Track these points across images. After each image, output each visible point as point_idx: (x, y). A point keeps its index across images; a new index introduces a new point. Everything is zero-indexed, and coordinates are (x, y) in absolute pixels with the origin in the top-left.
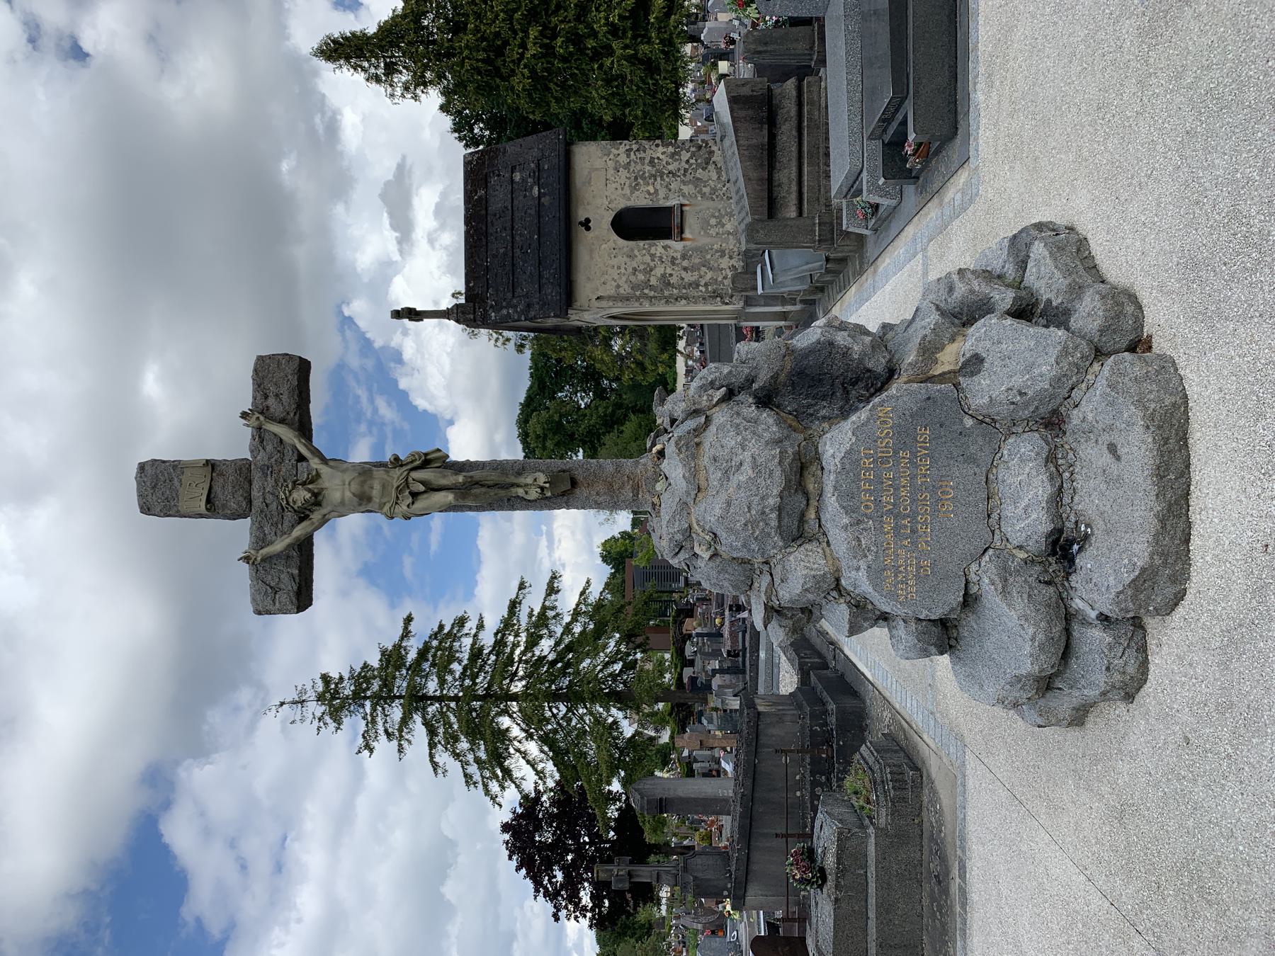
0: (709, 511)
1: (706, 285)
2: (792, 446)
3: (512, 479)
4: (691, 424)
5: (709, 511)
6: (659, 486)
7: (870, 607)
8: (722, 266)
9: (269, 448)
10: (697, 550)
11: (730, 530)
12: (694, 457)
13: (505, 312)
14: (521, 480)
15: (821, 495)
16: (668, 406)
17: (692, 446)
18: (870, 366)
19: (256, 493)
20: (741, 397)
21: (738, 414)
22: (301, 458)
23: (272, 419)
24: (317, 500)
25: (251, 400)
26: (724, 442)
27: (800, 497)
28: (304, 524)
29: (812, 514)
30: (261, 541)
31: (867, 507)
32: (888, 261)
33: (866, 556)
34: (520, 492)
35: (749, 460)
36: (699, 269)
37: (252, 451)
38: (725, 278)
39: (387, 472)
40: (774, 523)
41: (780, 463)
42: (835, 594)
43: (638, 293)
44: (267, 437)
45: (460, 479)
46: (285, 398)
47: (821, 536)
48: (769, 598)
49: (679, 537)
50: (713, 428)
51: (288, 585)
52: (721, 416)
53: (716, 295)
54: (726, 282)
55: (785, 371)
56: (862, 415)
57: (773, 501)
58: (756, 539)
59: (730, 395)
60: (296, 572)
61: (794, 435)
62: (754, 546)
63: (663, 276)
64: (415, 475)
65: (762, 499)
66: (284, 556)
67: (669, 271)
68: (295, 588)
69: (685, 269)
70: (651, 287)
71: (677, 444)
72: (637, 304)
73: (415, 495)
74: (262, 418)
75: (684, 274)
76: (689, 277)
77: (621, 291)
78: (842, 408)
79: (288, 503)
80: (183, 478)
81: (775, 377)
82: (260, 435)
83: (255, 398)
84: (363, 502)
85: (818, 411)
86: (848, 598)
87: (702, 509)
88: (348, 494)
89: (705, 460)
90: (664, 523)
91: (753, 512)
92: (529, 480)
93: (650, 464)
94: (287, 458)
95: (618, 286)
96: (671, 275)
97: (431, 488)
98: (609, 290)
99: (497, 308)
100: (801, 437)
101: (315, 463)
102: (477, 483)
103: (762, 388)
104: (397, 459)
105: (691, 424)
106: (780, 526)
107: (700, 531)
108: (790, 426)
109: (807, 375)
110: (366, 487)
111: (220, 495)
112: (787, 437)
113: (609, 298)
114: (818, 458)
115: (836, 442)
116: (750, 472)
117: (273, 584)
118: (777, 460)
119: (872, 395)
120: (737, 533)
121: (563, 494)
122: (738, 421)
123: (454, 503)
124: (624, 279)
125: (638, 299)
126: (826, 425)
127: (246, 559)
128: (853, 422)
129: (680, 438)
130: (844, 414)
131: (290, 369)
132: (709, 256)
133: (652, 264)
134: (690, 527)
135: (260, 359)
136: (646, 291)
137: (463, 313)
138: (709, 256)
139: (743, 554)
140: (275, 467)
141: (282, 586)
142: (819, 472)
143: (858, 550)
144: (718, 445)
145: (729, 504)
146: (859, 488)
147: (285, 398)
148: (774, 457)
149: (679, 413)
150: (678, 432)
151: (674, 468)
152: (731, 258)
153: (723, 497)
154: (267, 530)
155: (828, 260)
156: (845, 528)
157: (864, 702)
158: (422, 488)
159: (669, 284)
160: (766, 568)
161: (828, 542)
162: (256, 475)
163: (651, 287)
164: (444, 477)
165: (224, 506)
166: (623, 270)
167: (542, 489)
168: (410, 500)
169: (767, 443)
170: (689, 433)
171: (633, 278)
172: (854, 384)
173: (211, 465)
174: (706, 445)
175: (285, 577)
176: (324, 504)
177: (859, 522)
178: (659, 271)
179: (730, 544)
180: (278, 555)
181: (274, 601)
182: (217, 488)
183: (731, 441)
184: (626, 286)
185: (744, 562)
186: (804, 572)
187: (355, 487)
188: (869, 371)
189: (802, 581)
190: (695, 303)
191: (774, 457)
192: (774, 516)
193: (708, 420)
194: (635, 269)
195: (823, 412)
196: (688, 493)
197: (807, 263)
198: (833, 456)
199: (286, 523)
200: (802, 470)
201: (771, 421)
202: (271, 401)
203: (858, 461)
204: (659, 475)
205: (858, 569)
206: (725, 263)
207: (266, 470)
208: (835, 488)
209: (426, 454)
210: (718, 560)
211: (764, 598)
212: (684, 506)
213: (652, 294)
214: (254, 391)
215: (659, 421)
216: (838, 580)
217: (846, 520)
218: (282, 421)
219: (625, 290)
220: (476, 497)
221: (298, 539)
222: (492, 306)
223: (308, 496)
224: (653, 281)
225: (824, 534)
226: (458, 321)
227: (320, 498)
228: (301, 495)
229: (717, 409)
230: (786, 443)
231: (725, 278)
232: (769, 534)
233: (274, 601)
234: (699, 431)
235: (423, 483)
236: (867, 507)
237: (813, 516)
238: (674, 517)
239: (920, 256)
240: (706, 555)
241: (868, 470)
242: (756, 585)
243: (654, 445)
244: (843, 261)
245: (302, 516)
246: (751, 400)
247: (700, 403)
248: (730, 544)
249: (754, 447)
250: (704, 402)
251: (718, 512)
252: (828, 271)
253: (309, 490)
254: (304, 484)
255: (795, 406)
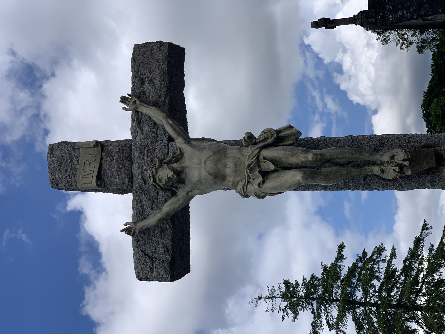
3: (366, 156)
9: (145, 129)
13: (400, 13)
14: (377, 157)
19: (136, 171)
22: (171, 139)
23: (146, 102)
24: (180, 177)
25: (130, 86)
28: (173, 200)
30: (139, 213)
34: (376, 170)
37: (132, 133)
39: (240, 150)
44: (143, 119)
45: (310, 157)
46: (157, 82)
51: (163, 256)
60: (169, 244)
64: (266, 153)
66: (158, 228)
68: (169, 258)
73: (265, 174)
74: (138, 102)
79: (154, 181)
80: (80, 157)
82: (138, 120)
83: (133, 84)
84: (218, 180)
88: (204, 173)
92: (386, 158)
94: (160, 138)
97: (282, 167)
99: (394, 11)
101: (179, 142)
102: (328, 161)
104: (250, 136)
110: (220, 166)
111: (110, 172)
117: (150, 254)
121: (427, 172)
123: (303, 182)
127: (128, 231)
131: (161, 55)
135: (137, 47)
137: (367, 18)
140: (150, 147)
141: (158, 256)
147: (157, 82)
154: (145, 204)
158: (272, 167)
162: (136, 155)
164: (294, 155)
165: (112, 182)
167: (401, 167)
168: (260, 179)
173: (102, 146)
175: (160, 248)
176: (187, 182)
180: (154, 228)
181: (151, 269)
182: (106, 167)
187: (210, 165)
199: (161, 198)
202: (147, 86)
207: (145, 149)
209: (278, 132)
214: (133, 78)
218: (155, 104)
220: (326, 177)
221: (167, 215)
222: (389, 10)
223: (171, 174)
226: (362, 25)
227: (183, 176)
228: (165, 173)
233: (151, 269)
235: (273, 161)
245: (171, 189)
253: (172, 169)
254: (170, 162)
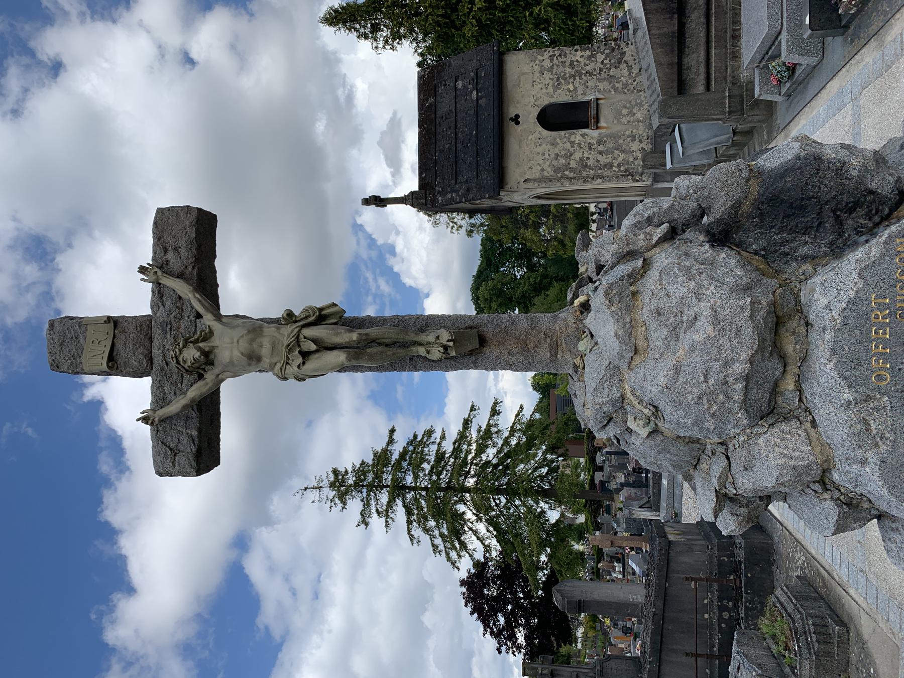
0: (650, 379)
1: (619, 166)
2: (765, 293)
3: (412, 337)
4: (624, 269)
5: (650, 379)
6: (582, 346)
7: (866, 505)
8: (633, 149)
9: (168, 303)
10: (631, 424)
11: (677, 404)
12: (630, 309)
13: (449, 196)
14: (423, 338)
15: (804, 359)
16: (593, 251)
17: (626, 296)
18: (873, 186)
19: (156, 351)
20: (688, 235)
21: (687, 254)
22: (199, 316)
23: (170, 274)
24: (208, 358)
25: (151, 254)
26: (671, 289)
27: (775, 362)
28: (200, 383)
29: (789, 385)
30: (160, 400)
31: (880, 378)
32: (803, 122)
33: (876, 445)
34: (422, 351)
35: (707, 312)
36: (613, 153)
37: (152, 308)
38: (636, 159)
39: (278, 329)
40: (738, 396)
41: (752, 316)
42: (817, 487)
43: (559, 175)
44: (166, 292)
45: (354, 336)
46: (183, 251)
47: (803, 414)
48: (723, 485)
49: (608, 408)
50: (654, 274)
51: (188, 448)
52: (663, 258)
53: (628, 174)
54: (636, 162)
55: (751, 198)
56: (871, 250)
57: (738, 368)
58: (713, 415)
59: (672, 235)
60: (195, 433)
61: (765, 280)
62: (710, 424)
63: (581, 159)
64: (307, 332)
65: (726, 365)
66: (183, 415)
67: (586, 155)
68: (194, 450)
69: (601, 153)
70: (571, 170)
71: (607, 293)
72: (559, 184)
73: (305, 355)
74: (159, 273)
75: (599, 157)
76: (603, 160)
77: (546, 173)
78: (832, 243)
79: (178, 362)
80: (88, 334)
81: (737, 206)
82: (159, 292)
83: (155, 252)
84: (253, 360)
85: (795, 249)
86: (836, 494)
87: (640, 376)
88: (236, 353)
89: (644, 314)
90: (589, 391)
91: (712, 382)
92: (431, 338)
93: (571, 321)
94: (186, 314)
95: (543, 170)
96: (588, 158)
97: (324, 347)
98: (535, 173)
99: (443, 193)
100: (775, 283)
101: (208, 319)
102: (373, 341)
103: (718, 221)
104: (290, 314)
105: (624, 269)
106: (745, 400)
107: (636, 402)
108: (758, 269)
109: (782, 201)
110: (255, 346)
111: (125, 353)
112: (758, 283)
113: (535, 180)
114: (799, 310)
115: (831, 290)
116: (709, 329)
117: (172, 446)
118: (747, 313)
119: (877, 225)
120: (687, 409)
121: (471, 353)
122: (688, 263)
123: (347, 363)
124: (548, 163)
125: (559, 180)
126: (808, 267)
127: (145, 420)
128: (859, 260)
129: (611, 286)
130: (837, 251)
131: (188, 221)
132: (621, 141)
133: (572, 150)
134: (623, 397)
135: (160, 211)
136: (566, 173)
137: (417, 199)
138: (621, 141)
139: (695, 433)
140: (174, 324)
141: (182, 448)
142: (803, 330)
143: (864, 436)
144: (662, 294)
145: (677, 370)
146: (868, 350)
147: (183, 251)
148: (743, 309)
149: (607, 258)
150: (607, 279)
151: (603, 324)
152: (641, 141)
153: (670, 361)
154: (167, 388)
155: (734, 132)
156: (847, 406)
157: (771, 538)
158: (313, 347)
159: (586, 166)
160: (721, 449)
161: (814, 423)
162: (157, 332)
163: (571, 170)
164: (337, 334)
165: (126, 364)
166: (547, 156)
167: (446, 348)
168: (300, 360)
169: (732, 290)
170: (622, 279)
171: (555, 163)
172: (851, 210)
173: (114, 322)
174: (646, 294)
175: (184, 439)
176: (216, 363)
177: (868, 398)
178: (578, 156)
179: (675, 420)
180: (178, 415)
181: (173, 463)
182: (119, 346)
183: (680, 288)
184: (549, 170)
185: (692, 441)
186: (781, 461)
187: (244, 345)
188: (871, 192)
189: (776, 473)
190: (609, 181)
191: (743, 309)
192: (739, 386)
193: (647, 264)
194: (557, 155)
195: (803, 250)
196: (621, 356)
197: (716, 136)
198: (828, 307)
199: (185, 382)
200: (780, 324)
201: (733, 262)
202: (170, 255)
203: (866, 313)
204: (582, 332)
205: (864, 462)
206: (635, 146)
207: (167, 327)
208: (833, 351)
209: (321, 310)
210: (659, 438)
211: (715, 483)
212: (614, 371)
213: (572, 175)
214: (154, 245)
215: (582, 269)
216: (826, 471)
217: (849, 396)
218: (180, 276)
219: (549, 172)
220: (371, 357)
221: (193, 400)
222: (439, 192)
223: (197, 354)
224: (573, 164)
225: (807, 410)
226: (413, 205)
227: (212, 357)
228: (191, 354)
229: (657, 250)
230: (757, 291)
231: (636, 159)
232: (730, 410)
233: (173, 463)
234: (634, 278)
235: (315, 341)
236: (880, 378)
237: (791, 387)
238: (601, 384)
239: (849, 108)
240: (644, 432)
241: (883, 326)
242: (704, 466)
243: (576, 296)
244: (749, 133)
245: (198, 372)
246: (702, 238)
247: (635, 243)
248: (675, 420)
249: (713, 296)
250: (641, 241)
251: (662, 380)
252: (734, 144)
253: (199, 349)
254: (196, 342)
255: (763, 243)
